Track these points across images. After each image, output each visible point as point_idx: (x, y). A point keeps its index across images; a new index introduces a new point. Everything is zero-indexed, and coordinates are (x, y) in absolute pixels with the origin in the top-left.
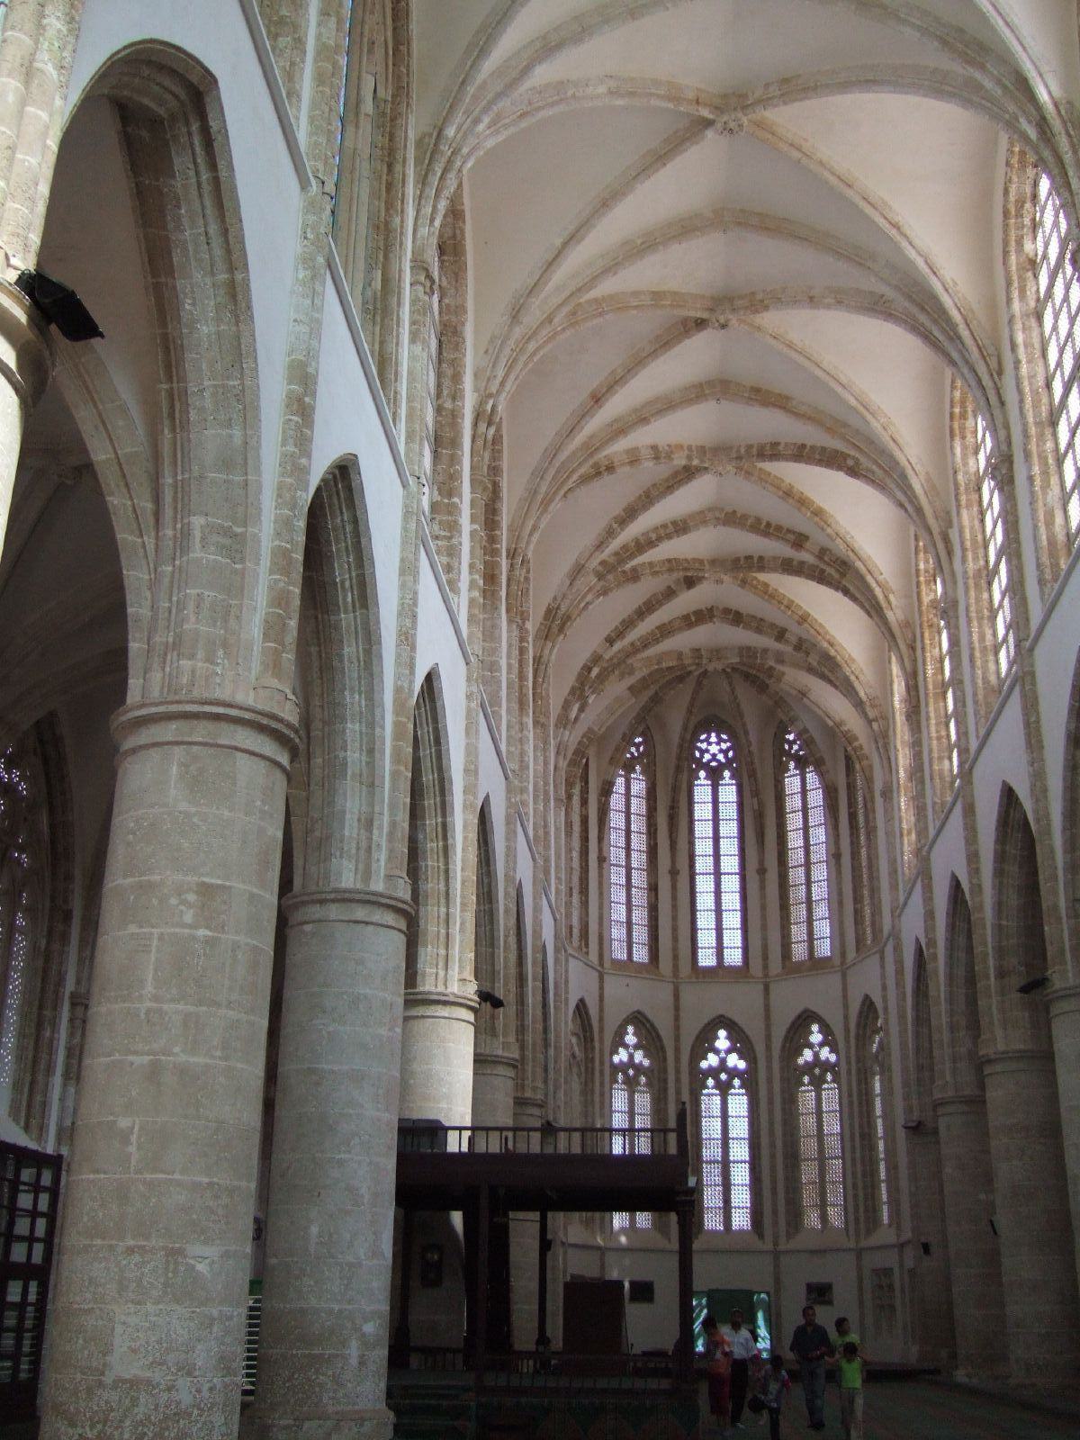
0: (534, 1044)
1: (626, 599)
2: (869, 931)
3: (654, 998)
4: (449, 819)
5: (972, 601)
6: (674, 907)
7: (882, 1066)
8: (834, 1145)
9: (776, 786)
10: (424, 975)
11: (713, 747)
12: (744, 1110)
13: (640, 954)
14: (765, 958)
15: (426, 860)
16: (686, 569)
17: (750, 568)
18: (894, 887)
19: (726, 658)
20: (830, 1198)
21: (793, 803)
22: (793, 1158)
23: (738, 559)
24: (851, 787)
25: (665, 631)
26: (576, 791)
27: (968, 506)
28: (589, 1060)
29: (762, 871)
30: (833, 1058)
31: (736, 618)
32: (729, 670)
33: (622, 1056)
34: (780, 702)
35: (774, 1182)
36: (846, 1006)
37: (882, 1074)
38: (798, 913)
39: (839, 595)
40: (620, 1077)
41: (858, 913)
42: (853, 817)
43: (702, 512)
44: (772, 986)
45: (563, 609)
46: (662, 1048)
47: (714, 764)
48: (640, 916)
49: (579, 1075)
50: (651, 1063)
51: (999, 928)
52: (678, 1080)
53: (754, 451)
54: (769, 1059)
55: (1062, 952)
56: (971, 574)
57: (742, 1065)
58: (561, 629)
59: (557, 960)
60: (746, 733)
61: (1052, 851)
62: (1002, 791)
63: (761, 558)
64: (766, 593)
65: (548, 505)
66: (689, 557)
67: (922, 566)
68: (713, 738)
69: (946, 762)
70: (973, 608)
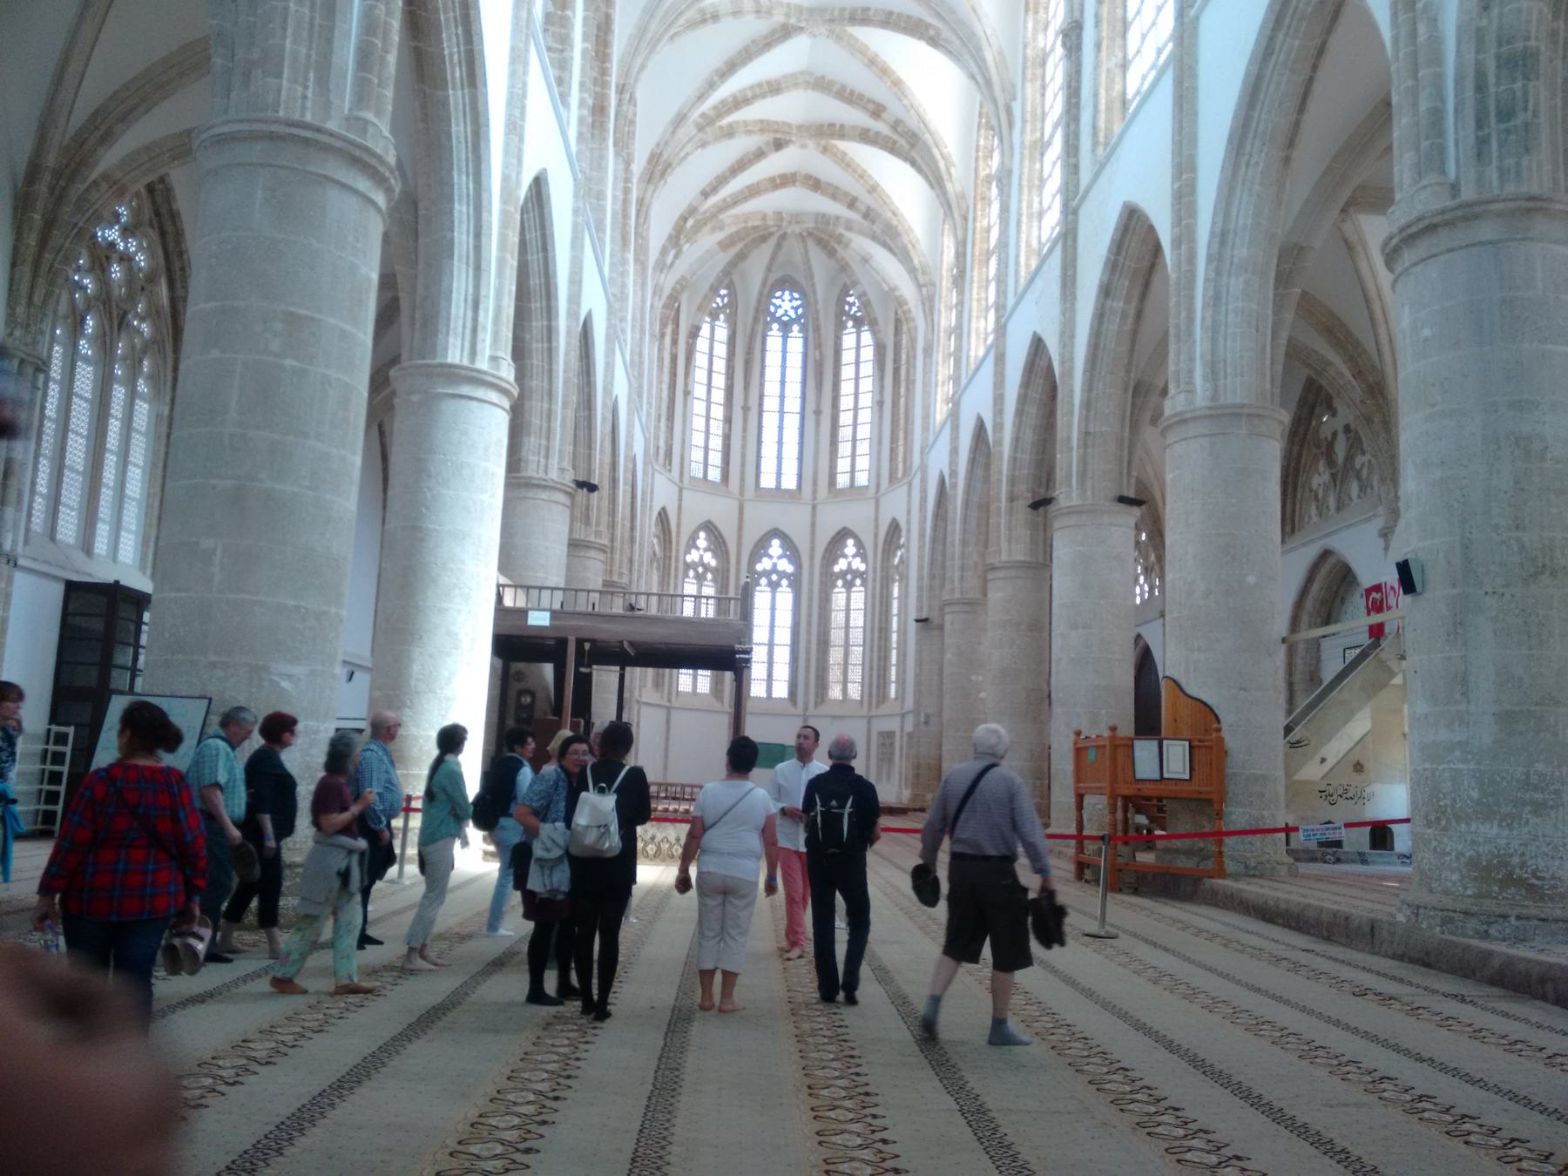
0: (622, 537)
1: (721, 155)
2: (900, 466)
3: (721, 511)
4: (553, 323)
5: (1026, 170)
6: (744, 438)
7: (901, 576)
8: (857, 636)
10: (527, 462)
11: (786, 304)
13: (715, 474)
14: (815, 484)
15: (531, 358)
16: (775, 131)
17: (832, 136)
18: (926, 428)
20: (851, 676)
21: (848, 357)
22: (824, 644)
23: (822, 126)
25: (753, 191)
26: (669, 331)
27: (1032, 81)
28: (667, 558)
29: (818, 412)
30: (862, 567)
31: (815, 184)
33: (693, 556)
34: (844, 267)
35: (808, 661)
36: (877, 526)
37: (901, 581)
38: (844, 449)
39: (906, 168)
40: (691, 573)
41: (893, 451)
42: (896, 371)
43: (794, 75)
44: (819, 508)
45: (665, 156)
46: (727, 552)
47: (785, 318)
48: (716, 443)
49: (658, 569)
51: (1014, 459)
53: (847, 15)
54: (812, 565)
55: (1069, 476)
56: (1027, 144)
57: (790, 569)
58: (663, 175)
59: (645, 472)
60: (815, 293)
61: (1072, 391)
62: (1032, 341)
63: (842, 126)
64: (843, 161)
65: (655, 45)
66: (780, 119)
67: (982, 142)
69: (983, 321)
70: (1025, 177)
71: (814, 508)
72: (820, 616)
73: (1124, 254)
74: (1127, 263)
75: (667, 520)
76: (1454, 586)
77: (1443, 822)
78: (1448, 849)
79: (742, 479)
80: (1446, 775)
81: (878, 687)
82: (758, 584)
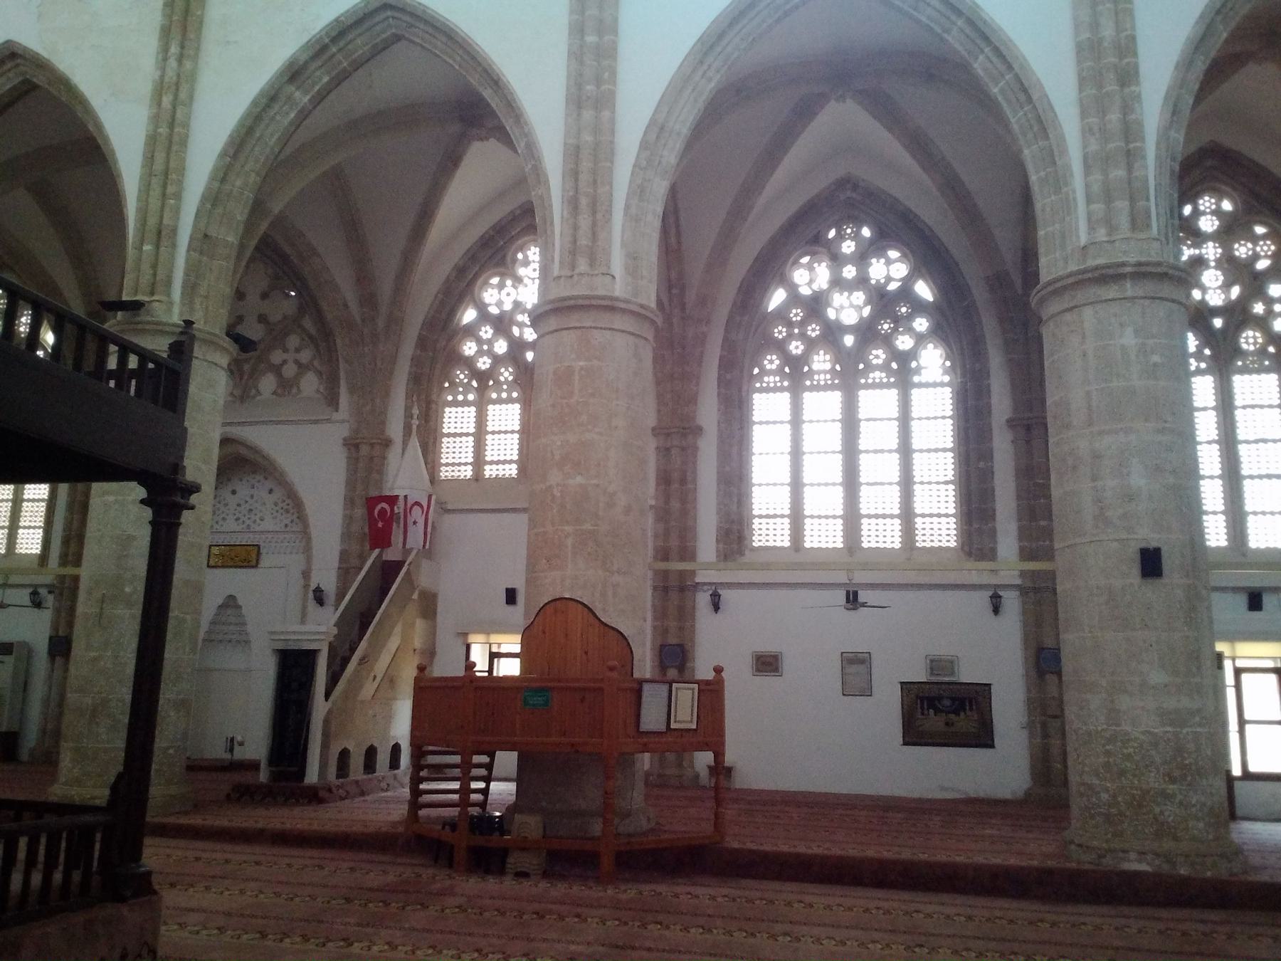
73: (342, 44)
74: (339, 57)
76: (1187, 576)
77: (1189, 778)
78: (1194, 802)
80: (1190, 737)
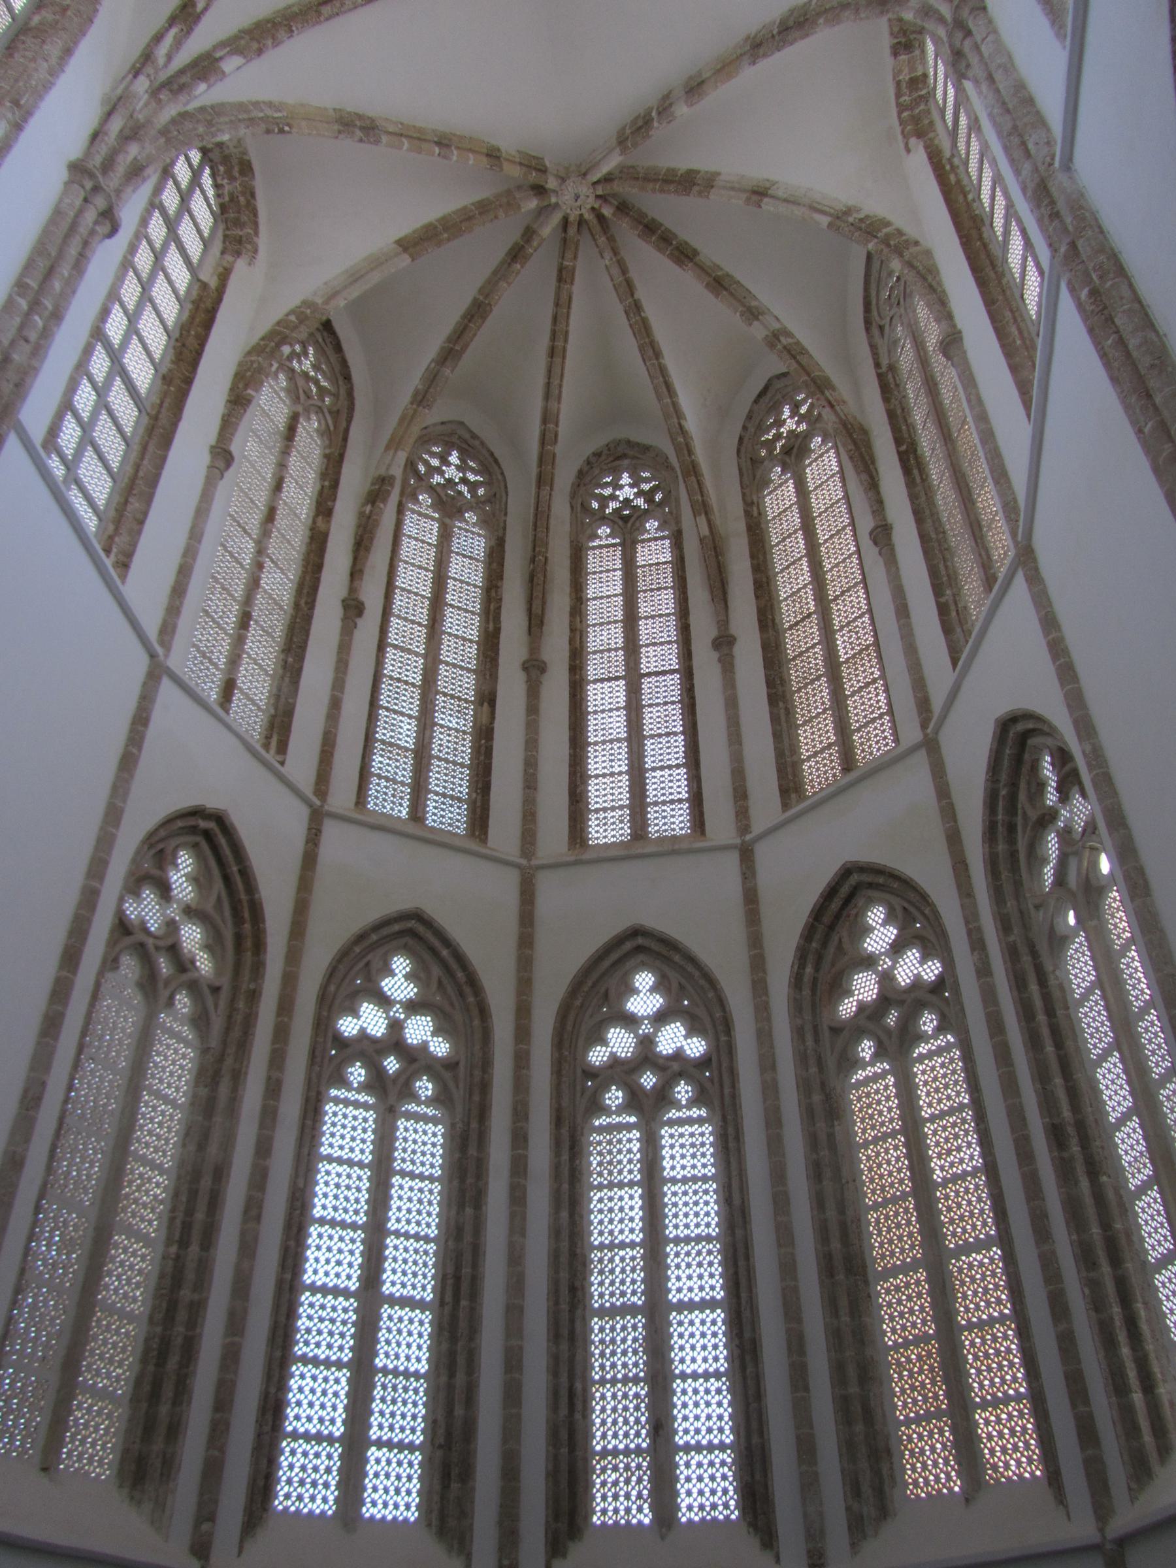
9: (748, 514)
12: (705, 1163)
14: (740, 794)
19: (595, 165)
20: (979, 1385)
24: (898, 419)
29: (724, 642)
32: (607, 211)
35: (796, 1344)
36: (949, 812)
40: (357, 1073)
44: (764, 854)
46: (483, 1012)
49: (200, 1021)
50: (454, 1046)
52: (521, 1084)
54: (762, 1010)
57: (696, 1047)
68: (625, 479)
71: (747, 855)
72: (816, 1172)
75: (246, 873)
79: (529, 815)
81: (1119, 1387)
82: (598, 1108)
